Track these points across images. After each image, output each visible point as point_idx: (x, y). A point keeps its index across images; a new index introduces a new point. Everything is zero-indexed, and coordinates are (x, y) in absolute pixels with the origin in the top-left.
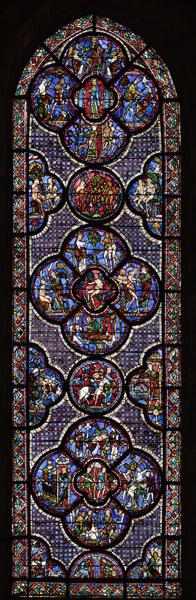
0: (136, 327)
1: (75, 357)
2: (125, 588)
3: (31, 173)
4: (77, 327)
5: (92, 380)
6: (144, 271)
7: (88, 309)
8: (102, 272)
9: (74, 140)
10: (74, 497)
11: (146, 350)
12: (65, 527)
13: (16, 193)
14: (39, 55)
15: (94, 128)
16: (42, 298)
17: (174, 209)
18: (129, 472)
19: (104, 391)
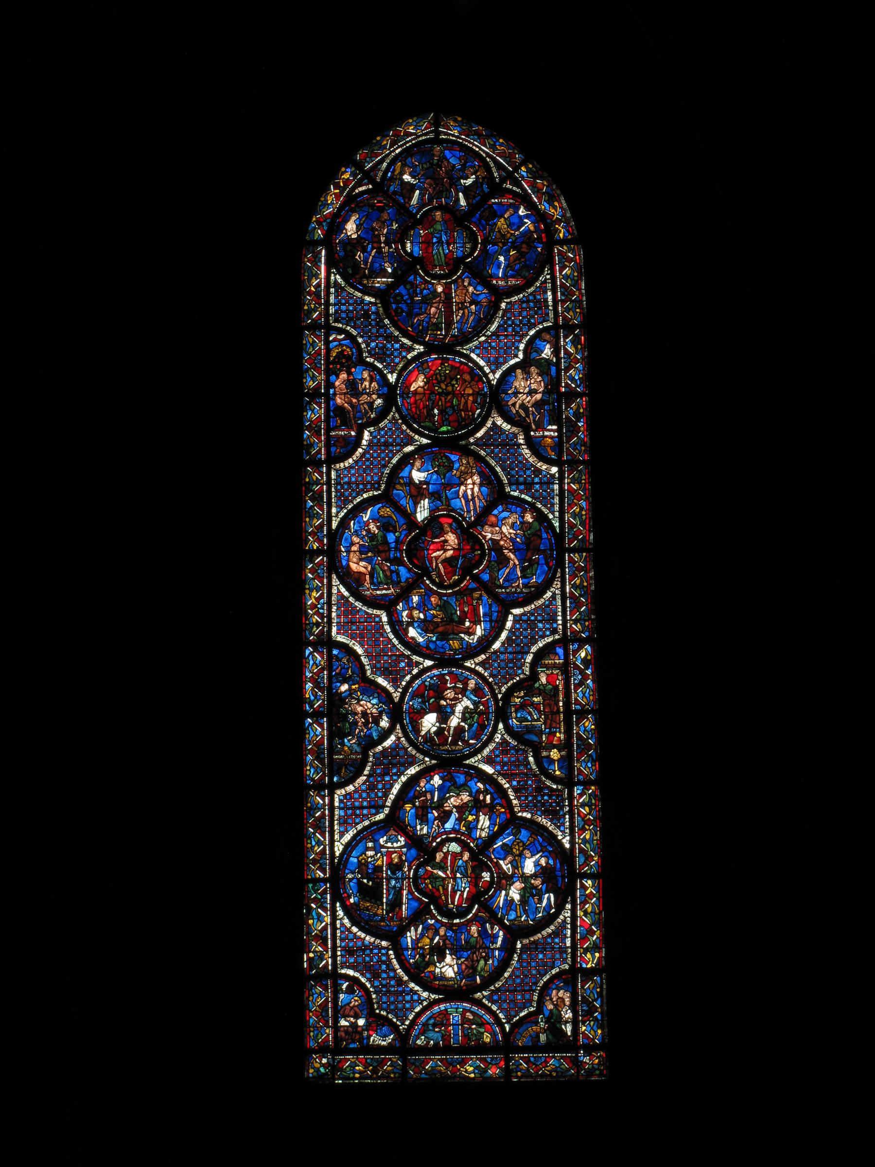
0: (517, 611)
1: (411, 664)
2: (507, 1065)
3: (334, 362)
4: (416, 613)
5: (443, 703)
6: (529, 518)
7: (433, 582)
8: (456, 520)
9: (404, 306)
10: (415, 904)
11: (534, 649)
12: (398, 957)
13: (308, 395)
14: (346, 176)
15: (440, 289)
16: (354, 566)
17: (577, 415)
18: (510, 858)
19: (464, 719)
